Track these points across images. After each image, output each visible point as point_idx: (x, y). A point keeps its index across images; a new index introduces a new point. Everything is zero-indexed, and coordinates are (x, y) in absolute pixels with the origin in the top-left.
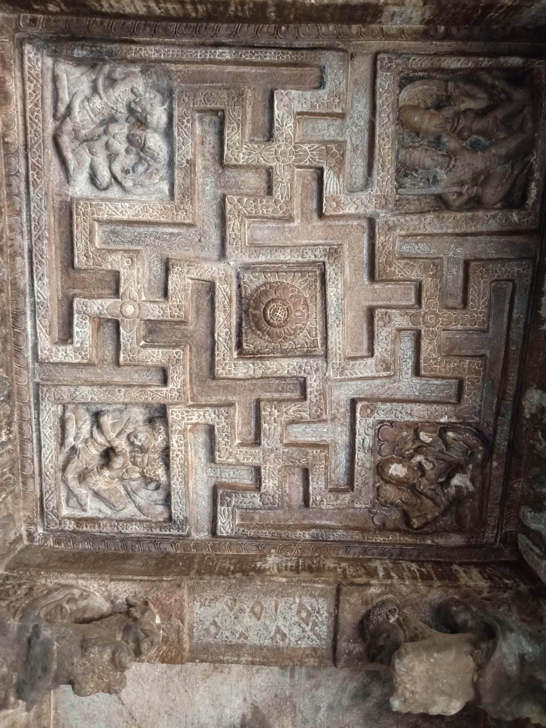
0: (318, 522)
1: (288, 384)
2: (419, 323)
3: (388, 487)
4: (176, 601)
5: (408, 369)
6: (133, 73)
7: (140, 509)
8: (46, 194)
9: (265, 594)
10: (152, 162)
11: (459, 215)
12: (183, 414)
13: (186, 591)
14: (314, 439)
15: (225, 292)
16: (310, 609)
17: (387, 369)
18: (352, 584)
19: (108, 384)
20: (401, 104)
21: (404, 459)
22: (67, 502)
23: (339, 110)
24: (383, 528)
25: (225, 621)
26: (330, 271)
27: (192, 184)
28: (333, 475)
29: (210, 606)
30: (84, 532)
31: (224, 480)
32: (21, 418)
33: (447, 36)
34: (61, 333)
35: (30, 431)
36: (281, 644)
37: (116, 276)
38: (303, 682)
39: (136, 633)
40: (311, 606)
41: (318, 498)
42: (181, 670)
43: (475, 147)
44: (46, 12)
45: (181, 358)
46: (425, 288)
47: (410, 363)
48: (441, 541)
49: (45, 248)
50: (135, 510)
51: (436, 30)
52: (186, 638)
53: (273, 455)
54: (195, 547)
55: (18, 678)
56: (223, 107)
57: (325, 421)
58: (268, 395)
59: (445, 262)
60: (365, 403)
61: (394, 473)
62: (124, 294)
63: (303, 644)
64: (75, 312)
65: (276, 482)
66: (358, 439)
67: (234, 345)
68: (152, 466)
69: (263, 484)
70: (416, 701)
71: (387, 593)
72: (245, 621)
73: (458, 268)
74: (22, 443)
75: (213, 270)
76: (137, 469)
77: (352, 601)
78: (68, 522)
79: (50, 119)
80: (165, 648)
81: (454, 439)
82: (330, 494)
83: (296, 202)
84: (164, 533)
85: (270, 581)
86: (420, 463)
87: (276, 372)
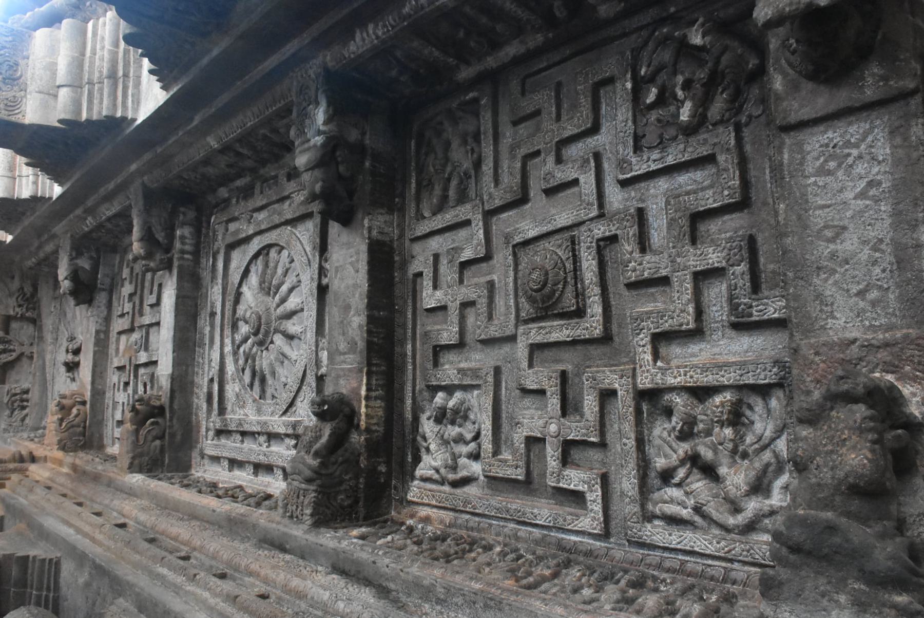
2: (551, 147)
3: (709, 115)
7: (779, 433)
9: (806, 227)
12: (643, 371)
15: (536, 334)
16: (822, 159)
17: (588, 161)
25: (853, 277)
26: (518, 239)
29: (832, 304)
32: (659, 567)
33: (403, 196)
35: (673, 560)
40: (818, 159)
41: (726, 193)
44: (389, 474)
49: (514, 507)
53: (679, 260)
55: (858, 579)
63: (883, 150)
65: (711, 250)
66: (654, 167)
69: (716, 265)
72: (850, 248)
76: (717, 430)
80: (908, 368)
81: (649, 66)
85: (786, 225)
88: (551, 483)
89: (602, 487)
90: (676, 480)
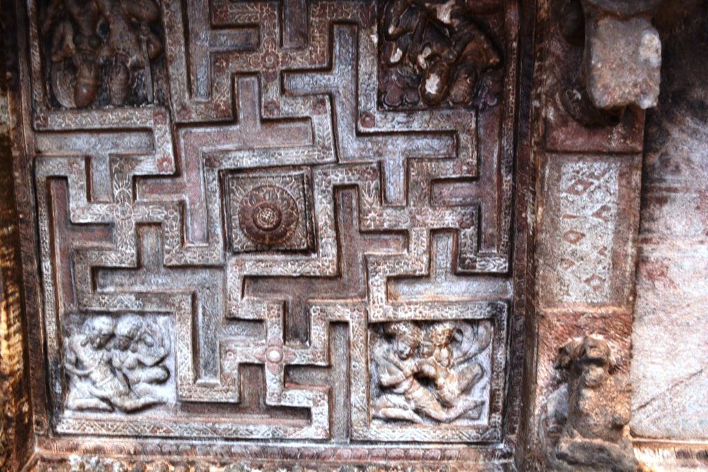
0: (495, 166)
1: (343, 202)
2: (274, 73)
3: (453, 93)
4: (559, 320)
5: (324, 79)
6: (70, 344)
7: (482, 349)
8: (175, 422)
9: (556, 229)
10: (142, 330)
11: (168, 41)
12: (376, 307)
13: (549, 311)
14: (402, 174)
15: (252, 265)
16: (573, 181)
17: (322, 102)
18: (544, 137)
19: (348, 376)
20: (74, 105)
21: (422, 77)
22: (473, 419)
23: (83, 163)
24: (501, 96)
25: (585, 270)
26: (226, 165)
27: (157, 295)
28: (442, 152)
29: (568, 286)
30: (504, 404)
31: (448, 265)
32: (385, 457)
33: (15, 69)
34: (302, 416)
35: (397, 450)
36: (613, 211)
37: (243, 366)
38: (684, 178)
39: (580, 362)
40: (570, 180)
41: (465, 168)
42: (664, 311)
43: (106, 29)
44: (30, 413)
45: (318, 307)
46: (239, 69)
47: (318, 76)
48: (514, 32)
49: (223, 426)
50: (484, 353)
51: (10, 79)
52: (603, 311)
53: (418, 217)
54: (520, 296)
56: (89, 268)
57: (380, 164)
58: (355, 222)
59: (215, 49)
60: (359, 123)
61: (435, 88)
62: (260, 359)
63: (614, 187)
64: (280, 404)
65: (448, 212)
66: (398, 128)
67: (304, 257)
68: (432, 337)
69: (450, 226)
70: (645, 81)
71: (554, 99)
73: (220, 35)
74: (407, 457)
75: (233, 277)
76: (437, 351)
77: (563, 137)
78: (493, 420)
79: (113, 416)
80: (612, 332)
81: (396, 26)
82: (461, 156)
83: (166, 198)
84: (505, 327)
85: (542, 224)
86: (426, 59)
87: (329, 216)
88: (271, 402)
89: (329, 402)
90: (400, 390)
